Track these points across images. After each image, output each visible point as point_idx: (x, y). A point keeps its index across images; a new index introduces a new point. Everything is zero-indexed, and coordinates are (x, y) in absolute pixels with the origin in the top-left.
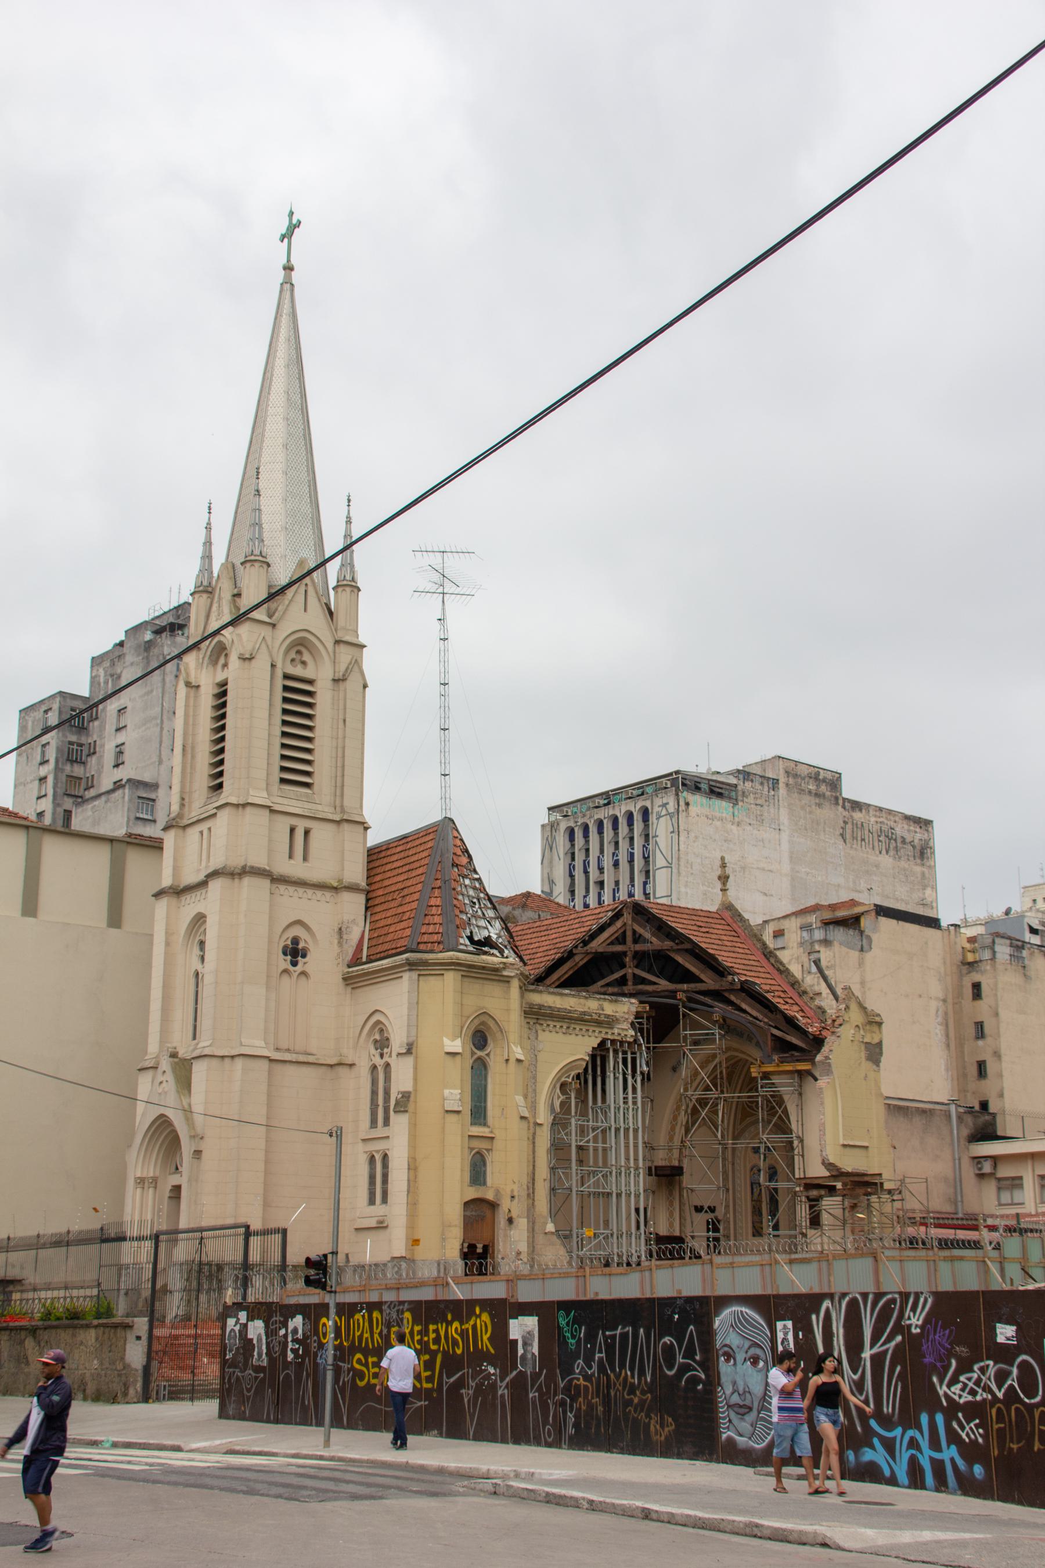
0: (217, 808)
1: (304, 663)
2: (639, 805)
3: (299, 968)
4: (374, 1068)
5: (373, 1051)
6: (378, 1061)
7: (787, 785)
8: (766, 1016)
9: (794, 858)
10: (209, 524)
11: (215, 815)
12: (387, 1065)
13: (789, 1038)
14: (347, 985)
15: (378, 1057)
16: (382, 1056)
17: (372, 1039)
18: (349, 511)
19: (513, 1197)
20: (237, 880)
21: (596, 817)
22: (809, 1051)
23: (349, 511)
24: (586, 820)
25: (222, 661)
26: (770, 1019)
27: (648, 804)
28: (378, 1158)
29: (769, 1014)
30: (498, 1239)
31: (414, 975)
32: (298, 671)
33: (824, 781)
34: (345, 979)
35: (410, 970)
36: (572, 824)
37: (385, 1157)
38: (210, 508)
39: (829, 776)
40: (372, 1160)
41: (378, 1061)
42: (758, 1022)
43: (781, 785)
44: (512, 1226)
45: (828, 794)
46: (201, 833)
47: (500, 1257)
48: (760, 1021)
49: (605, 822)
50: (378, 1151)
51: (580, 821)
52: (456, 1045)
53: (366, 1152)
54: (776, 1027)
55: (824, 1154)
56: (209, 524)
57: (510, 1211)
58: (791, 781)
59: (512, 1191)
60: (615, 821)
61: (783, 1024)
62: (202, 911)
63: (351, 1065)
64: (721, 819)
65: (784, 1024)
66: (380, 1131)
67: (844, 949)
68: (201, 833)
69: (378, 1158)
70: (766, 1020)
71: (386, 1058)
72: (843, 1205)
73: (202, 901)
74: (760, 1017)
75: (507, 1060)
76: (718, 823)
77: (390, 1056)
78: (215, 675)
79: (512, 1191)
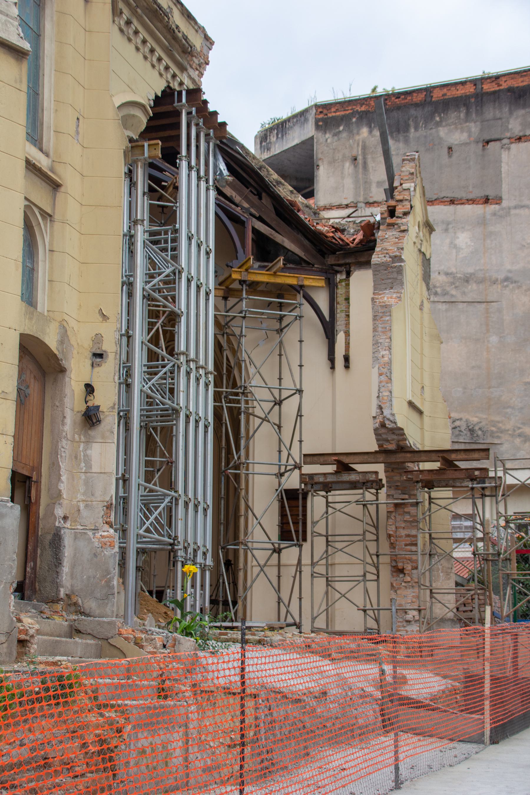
8: (246, 199)
13: (279, 238)
19: (99, 355)
22: (308, 263)
26: (252, 205)
29: (252, 197)
30: (55, 466)
42: (233, 206)
44: (92, 433)
47: (59, 512)
48: (237, 206)
54: (260, 219)
55: (386, 412)
57: (89, 389)
59: (98, 339)
61: (271, 216)
65: (273, 215)
70: (246, 205)
72: (430, 498)
74: (237, 199)
79: (98, 339)
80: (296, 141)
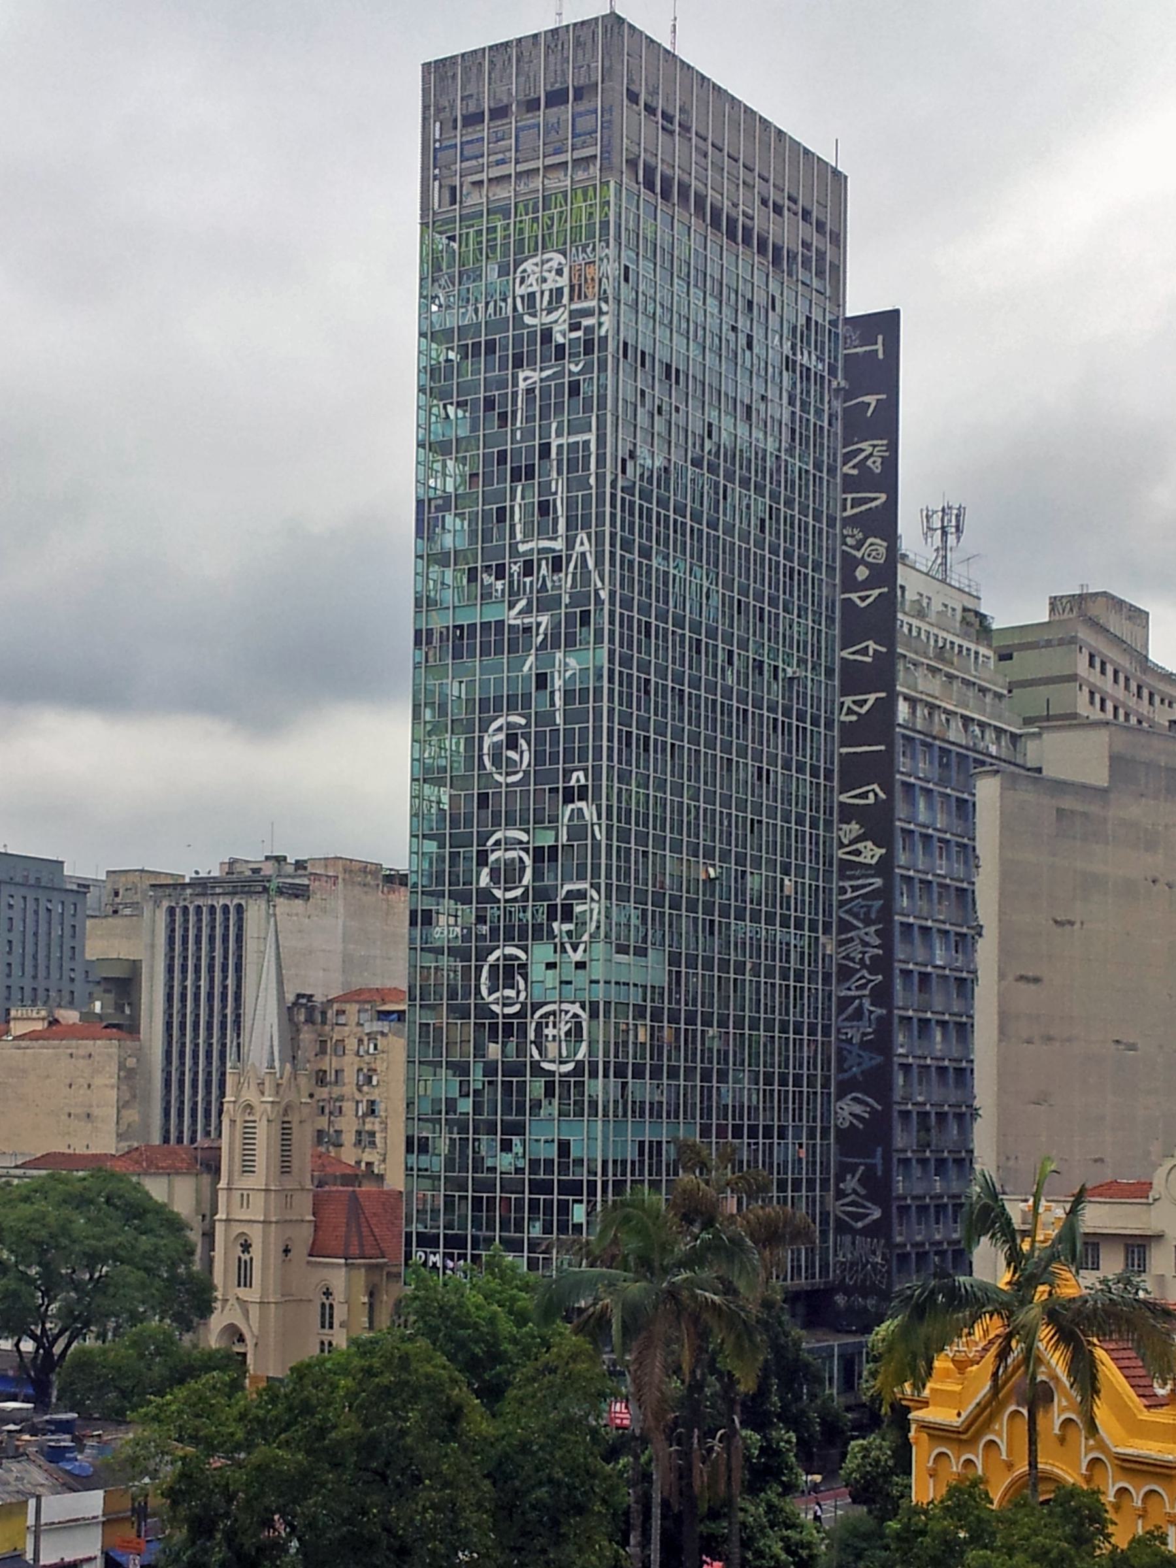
2: (236, 901)
4: (323, 1305)
7: (344, 880)
9: (345, 939)
12: (331, 1306)
21: (196, 903)
24: (186, 903)
27: (243, 902)
28: (326, 1343)
32: (286, 1119)
33: (370, 872)
36: (173, 904)
39: (373, 867)
40: (322, 1343)
43: (340, 880)
45: (372, 883)
46: (242, 1195)
49: (204, 909)
51: (182, 904)
52: (366, 1299)
58: (347, 876)
60: (212, 909)
64: (297, 915)
66: (326, 1331)
67: (395, 1038)
68: (242, 1195)
69: (326, 1343)
71: (330, 1300)
76: (295, 918)
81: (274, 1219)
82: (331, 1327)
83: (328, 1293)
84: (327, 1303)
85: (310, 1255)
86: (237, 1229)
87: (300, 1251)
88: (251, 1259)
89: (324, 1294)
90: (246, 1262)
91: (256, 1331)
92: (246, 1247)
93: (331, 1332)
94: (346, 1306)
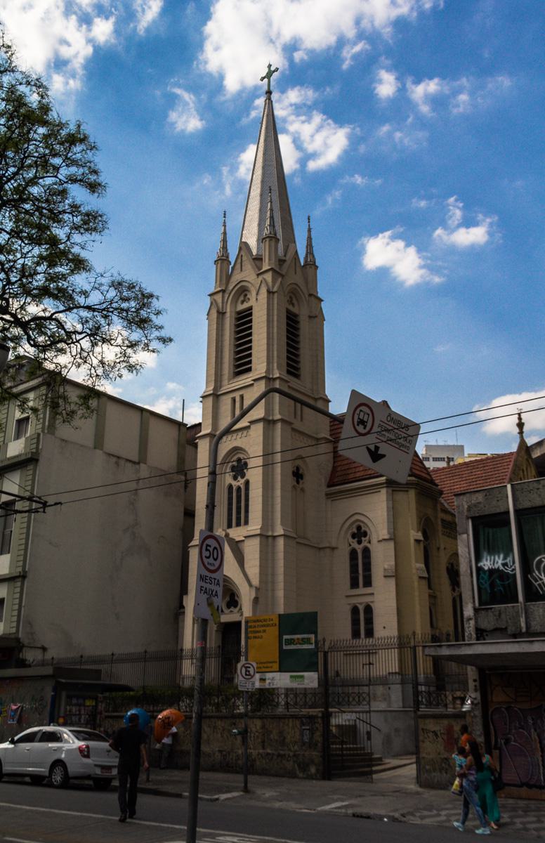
0: (254, 380)
1: (293, 305)
3: (301, 486)
5: (351, 540)
6: (355, 545)
10: (225, 223)
11: (252, 385)
14: (328, 498)
15: (356, 543)
16: (360, 542)
17: (350, 531)
18: (309, 225)
20: (271, 425)
23: (309, 225)
25: (242, 298)
28: (361, 608)
31: (390, 490)
34: (327, 495)
35: (386, 487)
37: (369, 610)
38: (225, 214)
41: (355, 545)
46: (234, 400)
50: (361, 604)
53: (349, 604)
56: (225, 223)
62: (239, 445)
63: (333, 549)
66: (361, 590)
68: (234, 400)
69: (361, 608)
71: (365, 544)
73: (238, 439)
75: (438, 549)
77: (370, 542)
78: (236, 307)
80: (539, 454)
81: (278, 417)
82: (368, 583)
83: (360, 533)
84: (359, 548)
85: (329, 486)
86: (227, 445)
87: (315, 479)
88: (247, 483)
89: (354, 536)
90: (239, 488)
91: (256, 582)
92: (240, 469)
93: (368, 590)
94: (391, 544)
